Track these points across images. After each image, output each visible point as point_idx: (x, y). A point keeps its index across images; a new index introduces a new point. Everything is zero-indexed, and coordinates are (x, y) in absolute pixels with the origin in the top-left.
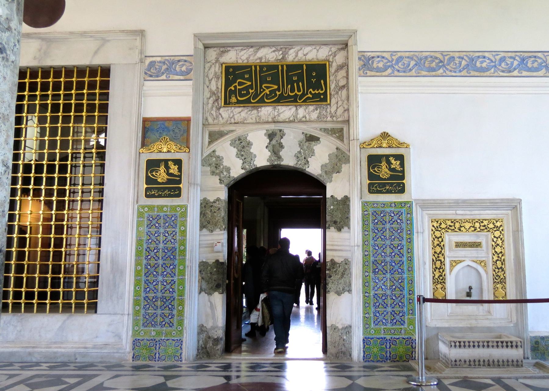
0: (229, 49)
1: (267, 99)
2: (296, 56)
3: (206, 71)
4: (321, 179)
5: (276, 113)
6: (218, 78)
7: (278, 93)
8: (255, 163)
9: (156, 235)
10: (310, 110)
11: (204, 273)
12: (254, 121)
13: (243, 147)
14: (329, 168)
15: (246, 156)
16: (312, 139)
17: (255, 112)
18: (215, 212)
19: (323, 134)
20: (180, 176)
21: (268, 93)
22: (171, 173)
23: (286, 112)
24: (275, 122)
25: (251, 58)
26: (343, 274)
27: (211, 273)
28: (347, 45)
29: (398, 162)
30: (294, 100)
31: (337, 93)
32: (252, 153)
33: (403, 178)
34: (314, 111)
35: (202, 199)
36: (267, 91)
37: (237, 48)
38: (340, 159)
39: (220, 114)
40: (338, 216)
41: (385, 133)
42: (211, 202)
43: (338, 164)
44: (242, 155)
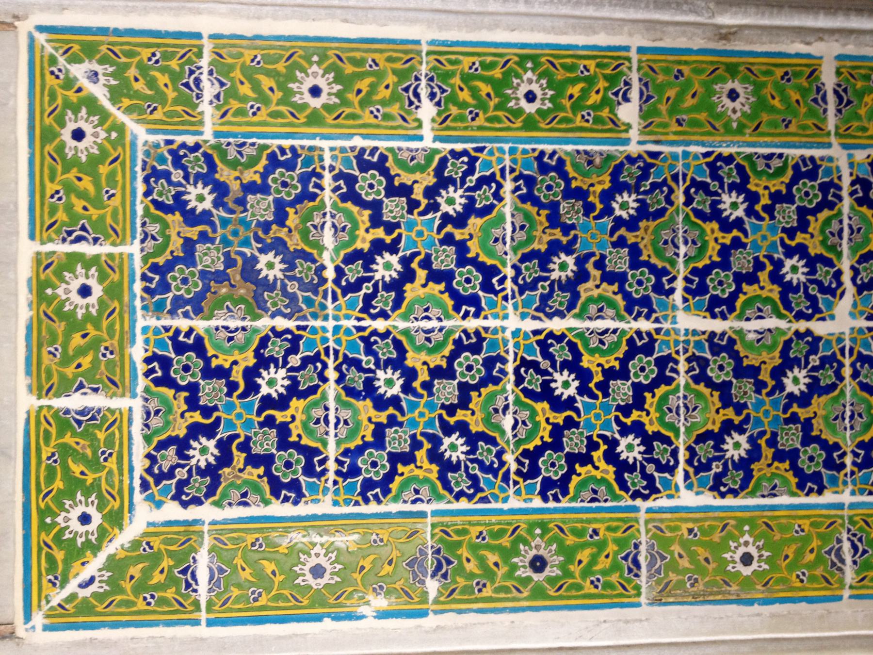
9: (389, 382)
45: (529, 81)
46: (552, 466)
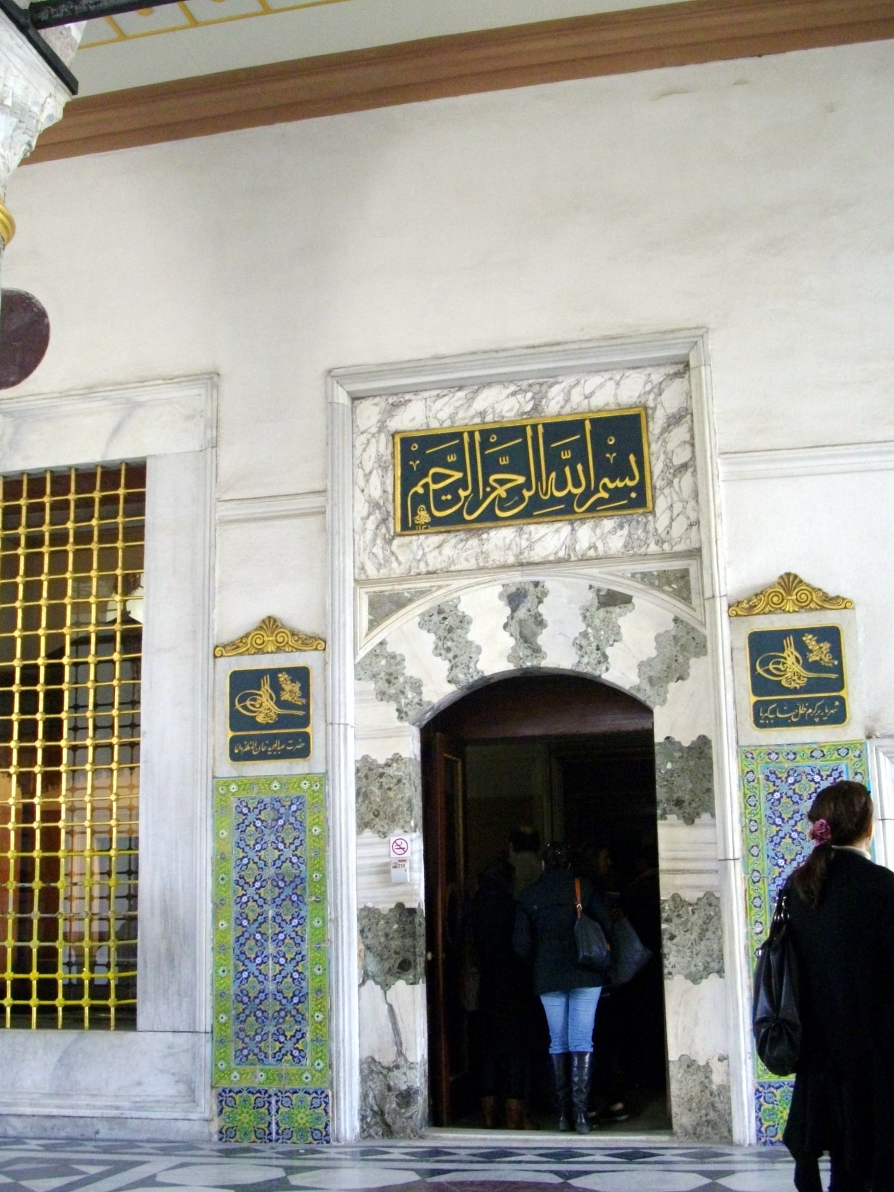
0: (407, 397)
1: (502, 509)
2: (567, 400)
3: (358, 452)
4: (640, 696)
5: (524, 544)
6: (385, 469)
7: (527, 494)
8: (480, 666)
10: (606, 530)
11: (370, 935)
12: (472, 564)
13: (450, 630)
14: (659, 667)
15: (458, 652)
16: (613, 600)
17: (474, 542)
18: (390, 789)
19: (640, 586)
20: (306, 707)
21: (504, 495)
22: (286, 701)
23: (548, 538)
24: (521, 565)
25: (461, 414)
26: (703, 932)
27: (387, 935)
28: (687, 365)
29: (826, 646)
30: (564, 509)
31: (670, 483)
32: (471, 643)
33: (840, 684)
34: (614, 531)
35: (359, 758)
36: (501, 491)
37: (426, 394)
38: (685, 646)
39: (393, 553)
40: (684, 787)
41: (788, 575)
42: (380, 766)
43: (681, 659)
44: (449, 650)
45: (319, 876)
46: (242, 882)
